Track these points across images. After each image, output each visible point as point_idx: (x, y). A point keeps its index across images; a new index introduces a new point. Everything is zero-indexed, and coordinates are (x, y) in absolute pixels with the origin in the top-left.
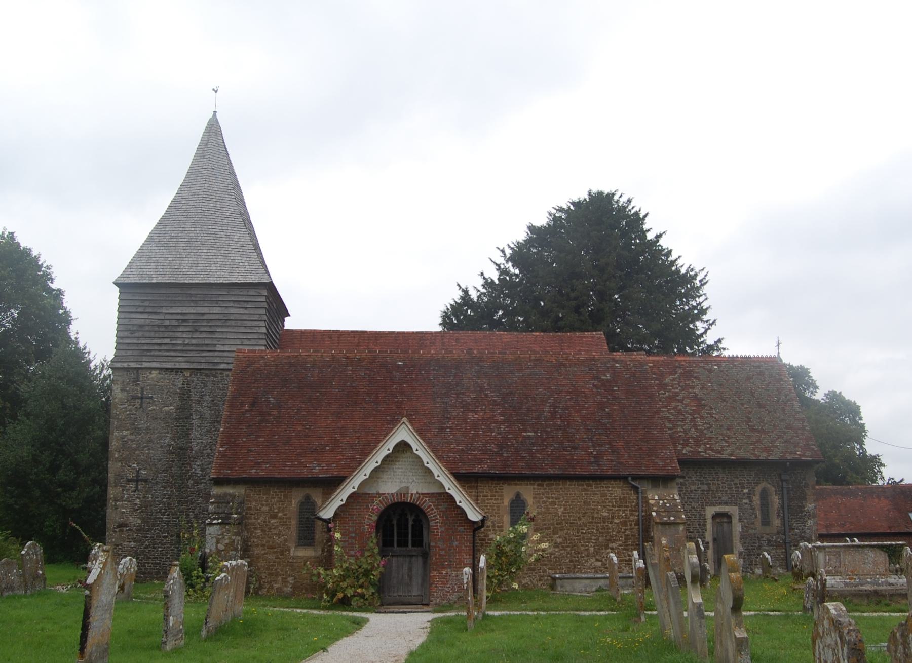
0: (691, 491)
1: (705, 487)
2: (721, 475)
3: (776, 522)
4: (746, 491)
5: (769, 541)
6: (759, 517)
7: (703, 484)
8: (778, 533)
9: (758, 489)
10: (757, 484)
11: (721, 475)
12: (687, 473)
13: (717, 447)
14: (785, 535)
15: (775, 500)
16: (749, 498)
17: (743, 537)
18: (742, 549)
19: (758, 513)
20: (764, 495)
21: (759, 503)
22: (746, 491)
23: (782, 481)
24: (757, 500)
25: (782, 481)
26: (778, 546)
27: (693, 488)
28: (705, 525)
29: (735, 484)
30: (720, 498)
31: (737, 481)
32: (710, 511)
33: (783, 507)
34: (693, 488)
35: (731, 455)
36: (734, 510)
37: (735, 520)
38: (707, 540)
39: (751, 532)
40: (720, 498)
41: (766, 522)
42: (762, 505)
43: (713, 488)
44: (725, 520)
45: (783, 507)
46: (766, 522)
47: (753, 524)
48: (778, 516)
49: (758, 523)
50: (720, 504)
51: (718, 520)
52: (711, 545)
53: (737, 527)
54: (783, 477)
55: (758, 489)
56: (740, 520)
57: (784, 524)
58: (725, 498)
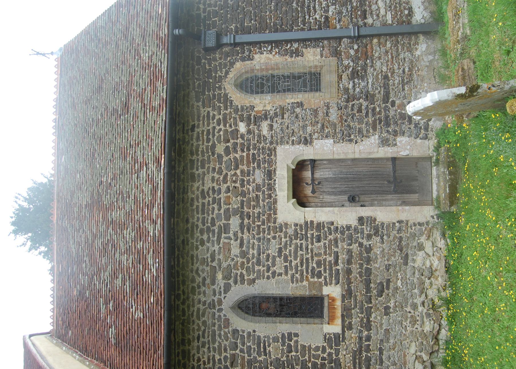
0: (244, 254)
1: (235, 222)
2: (209, 184)
3: (311, 58)
4: (242, 128)
5: (355, 75)
6: (299, 97)
7: (226, 228)
8: (336, 53)
9: (239, 98)
10: (227, 100)
11: (209, 184)
12: (204, 261)
13: (147, 189)
14: (340, 38)
15: (264, 60)
16: (257, 120)
17: (347, 136)
18: (374, 139)
19: (290, 99)
20: (255, 85)
21: (268, 98)
22: (242, 128)
23: (219, 45)
24: (263, 103)
25: (219, 45)
26: (366, 55)
27: (235, 251)
28: (320, 226)
29: (227, 151)
30: (258, 188)
31: (220, 149)
32: (288, 212)
33: (277, 43)
34: (235, 251)
35: (158, 162)
36: (286, 157)
37: (307, 153)
38: (354, 223)
39: (334, 115)
40: (258, 188)
41: (312, 81)
42: (274, 89)
43: (235, 203)
44: (307, 174)
45: (277, 43)
46: (312, 81)
47: (315, 112)
48: (297, 53)
49: (311, 99)
50: (271, 188)
51: (308, 191)
52: (366, 212)
53: (324, 148)
54: (211, 42)
55: (239, 98)
56: (307, 141)
57: (316, 41)
58: (259, 176)
